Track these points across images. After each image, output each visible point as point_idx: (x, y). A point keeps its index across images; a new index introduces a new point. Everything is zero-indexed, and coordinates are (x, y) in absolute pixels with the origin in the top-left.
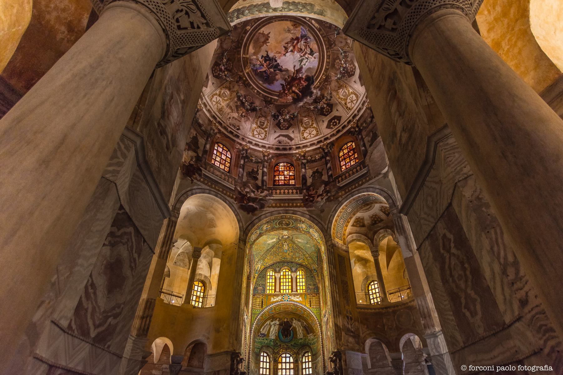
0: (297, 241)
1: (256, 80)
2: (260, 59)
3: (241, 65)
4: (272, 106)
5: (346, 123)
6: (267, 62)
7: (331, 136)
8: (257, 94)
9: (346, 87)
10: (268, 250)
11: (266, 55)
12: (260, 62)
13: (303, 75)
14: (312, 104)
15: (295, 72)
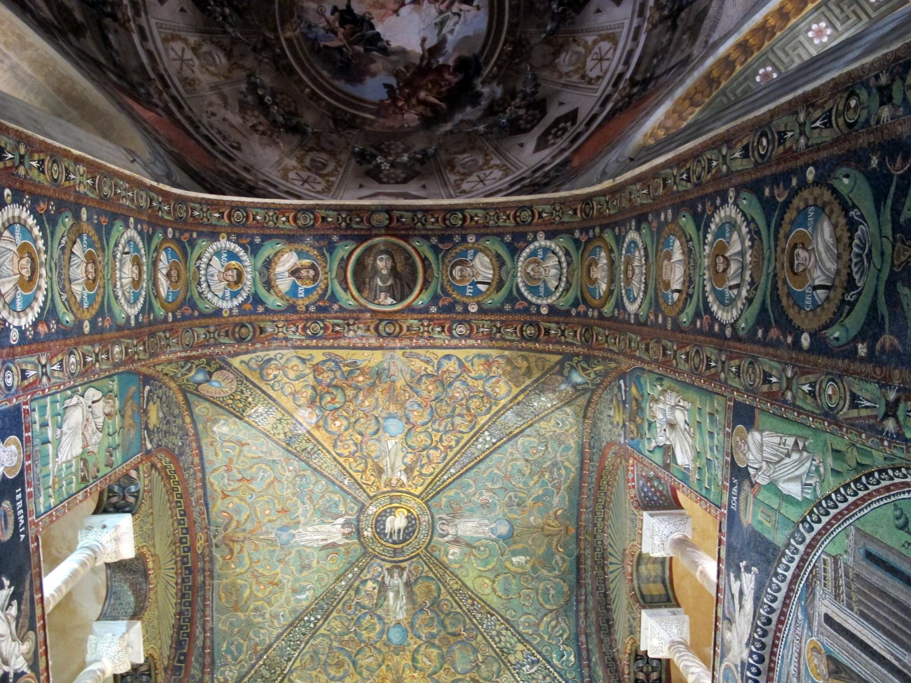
0: (457, 541)
1: (312, 65)
2: (328, 14)
3: (274, 13)
4: (356, 132)
5: (597, 108)
6: (348, 27)
7: (554, 158)
8: (310, 98)
9: (575, 41)
10: (298, 620)
11: (344, 8)
12: (328, 21)
13: (449, 58)
14: (480, 120)
15: (427, 55)
